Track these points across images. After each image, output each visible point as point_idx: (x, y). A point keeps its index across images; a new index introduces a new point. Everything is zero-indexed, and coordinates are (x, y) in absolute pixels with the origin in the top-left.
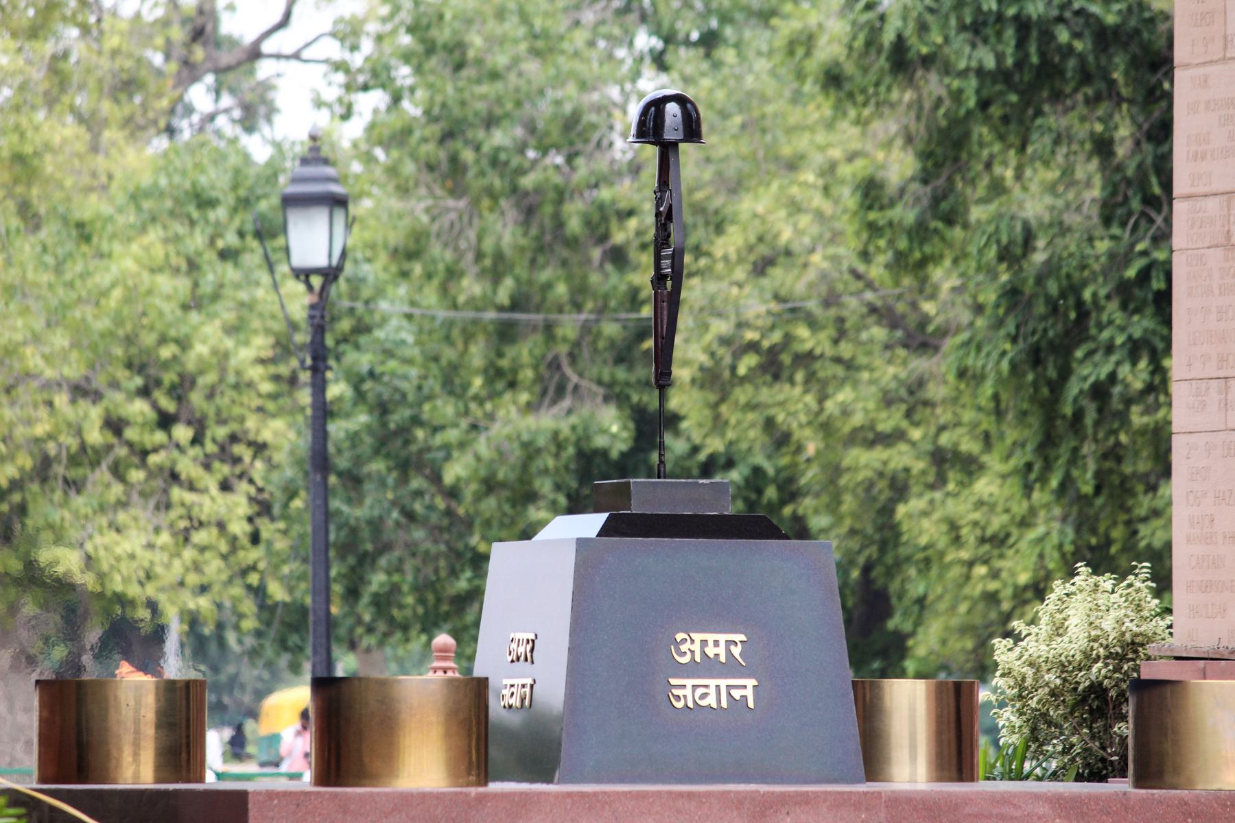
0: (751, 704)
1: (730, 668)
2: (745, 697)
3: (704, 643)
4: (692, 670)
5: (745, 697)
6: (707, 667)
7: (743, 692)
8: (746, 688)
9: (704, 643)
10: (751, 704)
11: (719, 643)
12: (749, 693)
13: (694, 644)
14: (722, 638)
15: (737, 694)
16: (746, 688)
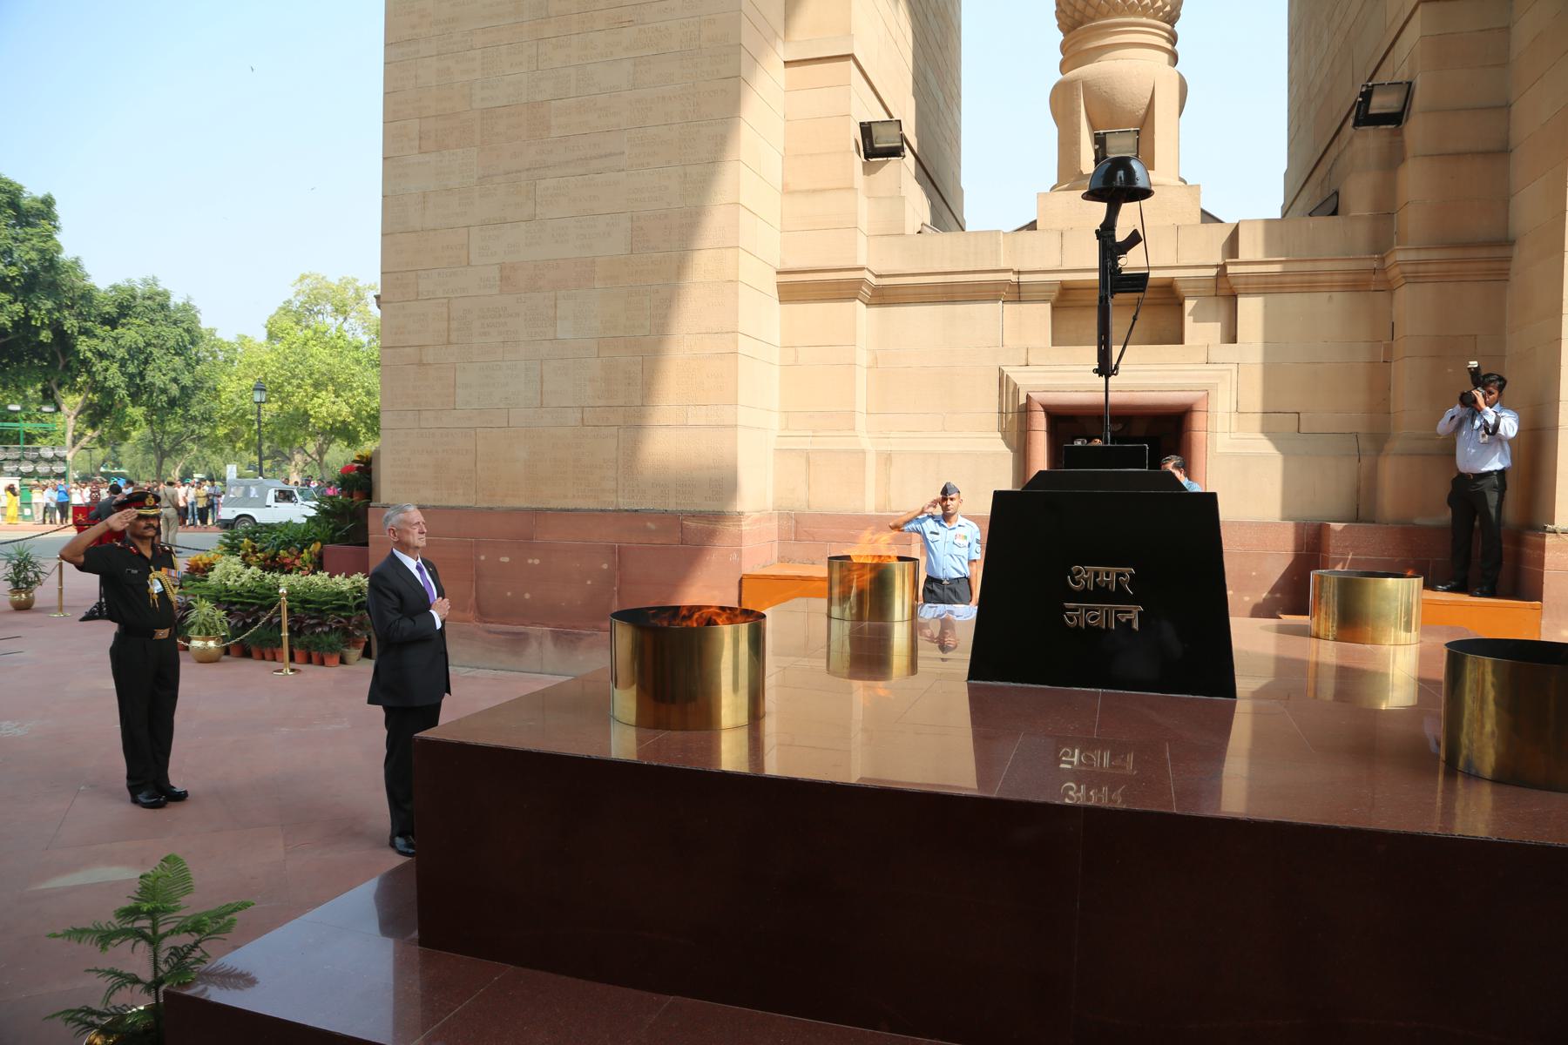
0: (1136, 626)
1: (1119, 596)
2: (1130, 621)
3: (1097, 575)
4: (1084, 596)
5: (1130, 621)
6: (1099, 594)
7: (1128, 616)
8: (1133, 614)
9: (1097, 575)
10: (1136, 626)
11: (1109, 575)
12: (1134, 616)
13: (1085, 575)
14: (1114, 570)
15: (1124, 618)
16: (1133, 614)
